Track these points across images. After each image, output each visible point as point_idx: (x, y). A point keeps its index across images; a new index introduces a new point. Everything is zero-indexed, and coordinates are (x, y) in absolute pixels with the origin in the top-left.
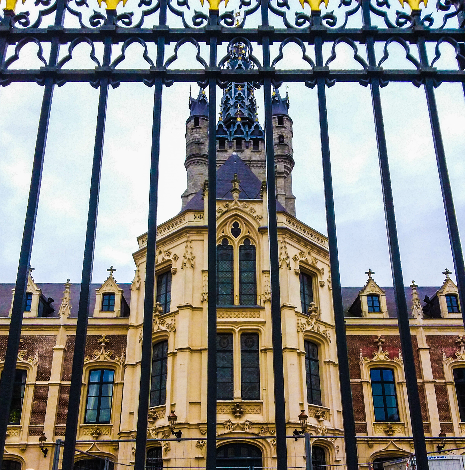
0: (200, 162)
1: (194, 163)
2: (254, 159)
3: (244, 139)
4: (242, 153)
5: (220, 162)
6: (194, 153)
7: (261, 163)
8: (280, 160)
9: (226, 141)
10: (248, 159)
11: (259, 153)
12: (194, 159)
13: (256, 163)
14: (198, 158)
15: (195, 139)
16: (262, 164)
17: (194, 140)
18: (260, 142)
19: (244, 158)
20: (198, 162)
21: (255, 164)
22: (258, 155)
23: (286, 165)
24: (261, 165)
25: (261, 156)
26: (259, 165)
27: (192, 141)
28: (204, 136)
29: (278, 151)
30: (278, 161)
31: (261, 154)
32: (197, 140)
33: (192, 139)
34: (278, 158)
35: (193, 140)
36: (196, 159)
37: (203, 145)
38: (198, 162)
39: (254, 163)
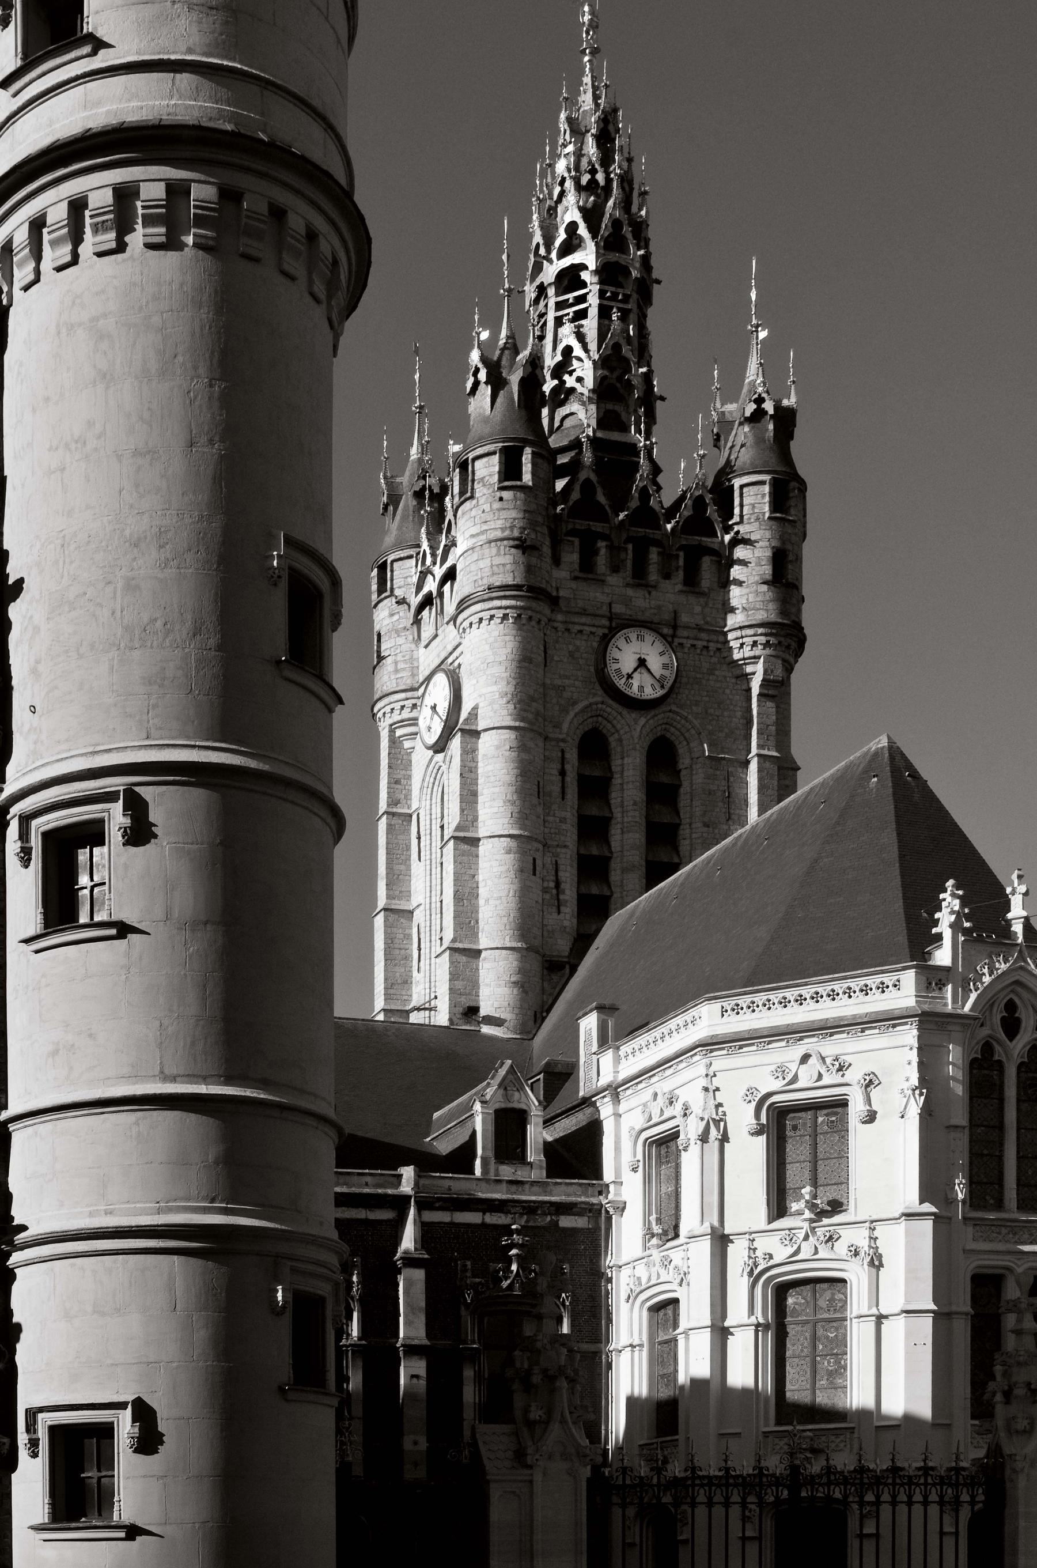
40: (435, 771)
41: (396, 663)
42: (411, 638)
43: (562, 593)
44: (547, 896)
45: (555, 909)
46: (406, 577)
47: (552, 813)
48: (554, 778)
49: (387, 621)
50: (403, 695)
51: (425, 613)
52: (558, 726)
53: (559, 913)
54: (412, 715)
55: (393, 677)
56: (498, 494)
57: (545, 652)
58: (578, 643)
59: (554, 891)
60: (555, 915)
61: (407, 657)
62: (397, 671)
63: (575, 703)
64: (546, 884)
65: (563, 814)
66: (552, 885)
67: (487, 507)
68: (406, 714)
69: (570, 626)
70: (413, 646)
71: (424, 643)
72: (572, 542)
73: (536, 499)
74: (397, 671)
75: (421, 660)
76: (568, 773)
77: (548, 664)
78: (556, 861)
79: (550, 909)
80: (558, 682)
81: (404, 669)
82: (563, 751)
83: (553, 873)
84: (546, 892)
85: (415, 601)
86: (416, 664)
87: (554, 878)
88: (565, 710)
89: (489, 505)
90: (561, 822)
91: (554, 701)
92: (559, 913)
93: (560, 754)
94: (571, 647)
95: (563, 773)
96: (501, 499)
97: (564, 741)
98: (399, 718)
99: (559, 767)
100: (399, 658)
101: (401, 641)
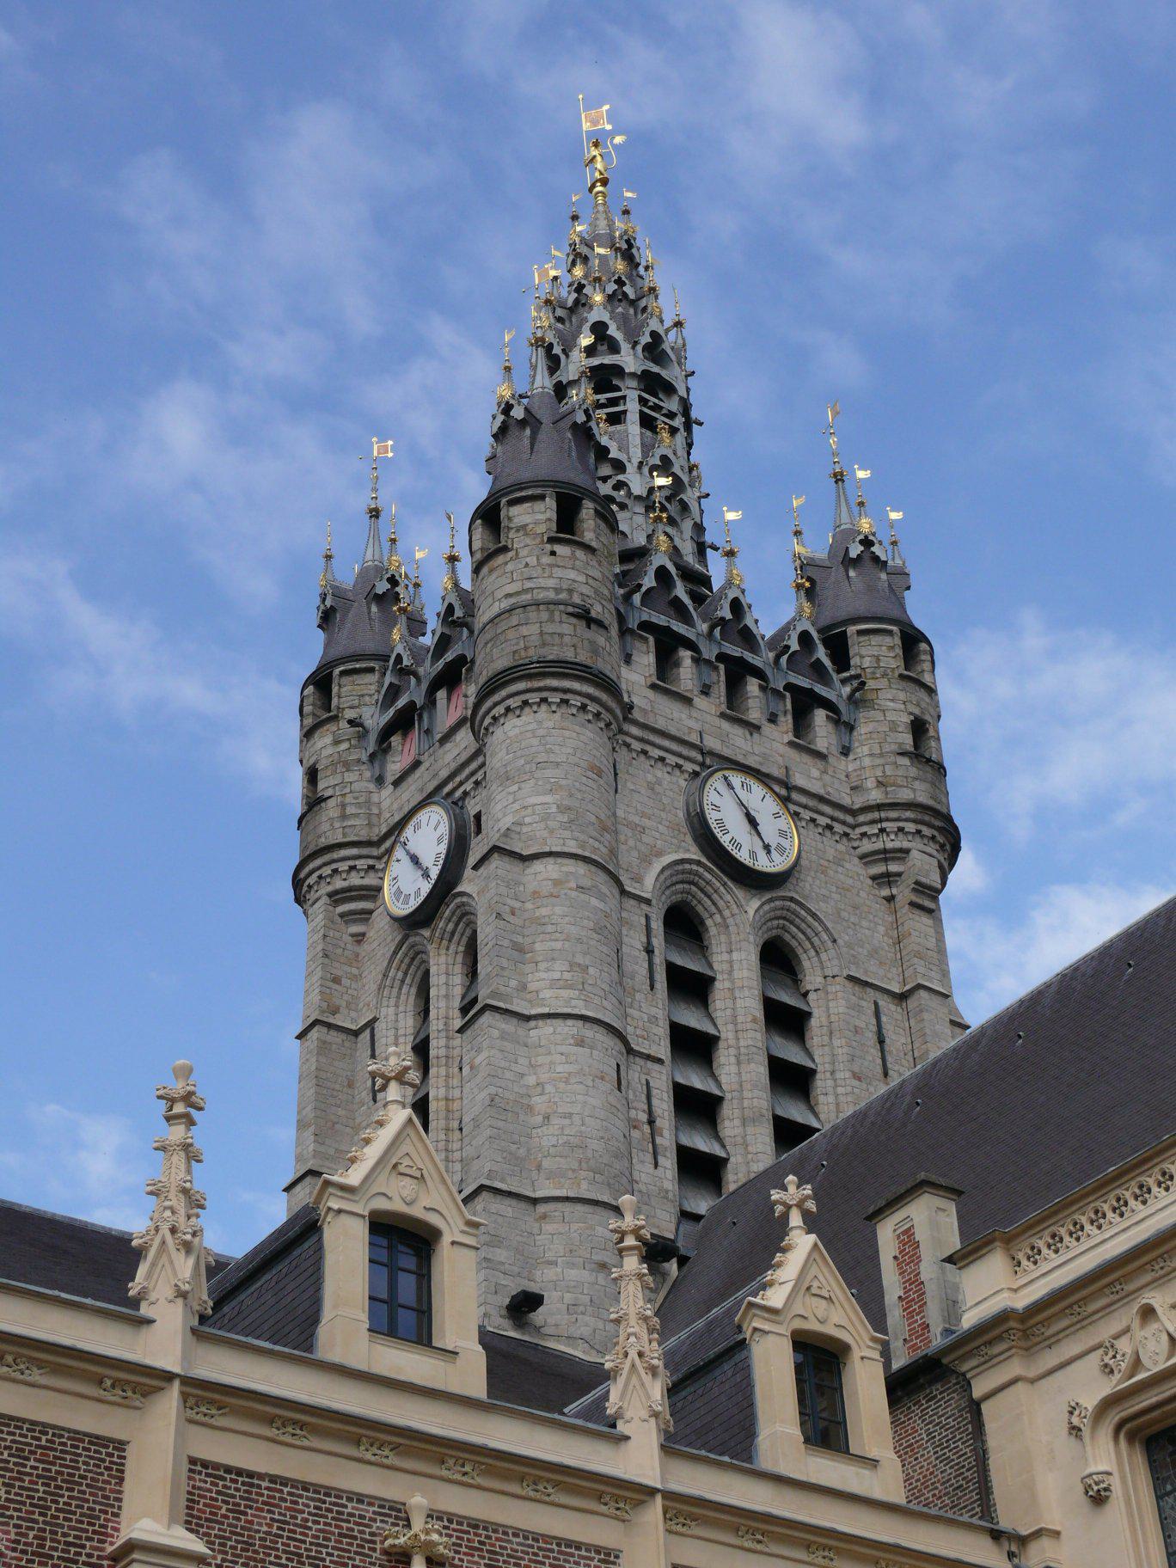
0: (593, 707)
1: (565, 702)
2: (799, 780)
3: (758, 673)
4: (751, 734)
5: (666, 743)
6: (569, 655)
7: (827, 809)
8: (926, 831)
9: (685, 655)
10: (776, 772)
11: (820, 764)
12: (567, 684)
13: (812, 803)
14: (590, 690)
15: (570, 591)
16: (833, 819)
17: (564, 596)
18: (820, 716)
19: (761, 764)
20: (583, 708)
21: (805, 807)
22: (815, 773)
23: (943, 861)
24: (829, 821)
25: (827, 778)
26: (823, 821)
27: (551, 595)
28: (606, 592)
29: (917, 784)
30: (919, 832)
31: (825, 772)
32: (577, 599)
33: (551, 583)
34: (920, 817)
35: (557, 590)
36: (576, 686)
37: (602, 631)
38: (583, 708)
39: (803, 800)
40: (407, 960)
41: (343, 806)
42: (368, 774)
43: (636, 700)
44: (636, 1134)
45: (649, 1158)
46: (363, 696)
47: (636, 1005)
48: (637, 953)
49: (329, 751)
50: (354, 851)
51: (395, 740)
52: (638, 879)
53: (656, 1165)
54: (370, 880)
55: (337, 825)
56: (548, 547)
57: (616, 774)
58: (659, 774)
59: (647, 1128)
60: (650, 1167)
61: (362, 800)
62: (344, 817)
63: (660, 854)
64: (633, 1113)
65: (654, 1011)
66: (644, 1117)
67: (532, 561)
68: (355, 880)
69: (648, 748)
70: (372, 787)
71: (390, 778)
72: (646, 639)
73: (600, 565)
74: (344, 817)
75: (385, 805)
76: (657, 952)
77: (619, 791)
78: (648, 1083)
79: (641, 1154)
80: (636, 819)
81: (356, 815)
82: (647, 918)
83: (644, 1098)
84: (635, 1127)
85: (375, 719)
86: (375, 811)
87: (646, 1107)
88: (646, 860)
89: (535, 558)
90: (649, 1021)
91: (631, 843)
92: (656, 1165)
93: (643, 921)
94: (650, 777)
95: (649, 951)
96: (553, 553)
97: (648, 902)
98: (345, 884)
99: (644, 939)
100: (349, 799)
101: (350, 777)
